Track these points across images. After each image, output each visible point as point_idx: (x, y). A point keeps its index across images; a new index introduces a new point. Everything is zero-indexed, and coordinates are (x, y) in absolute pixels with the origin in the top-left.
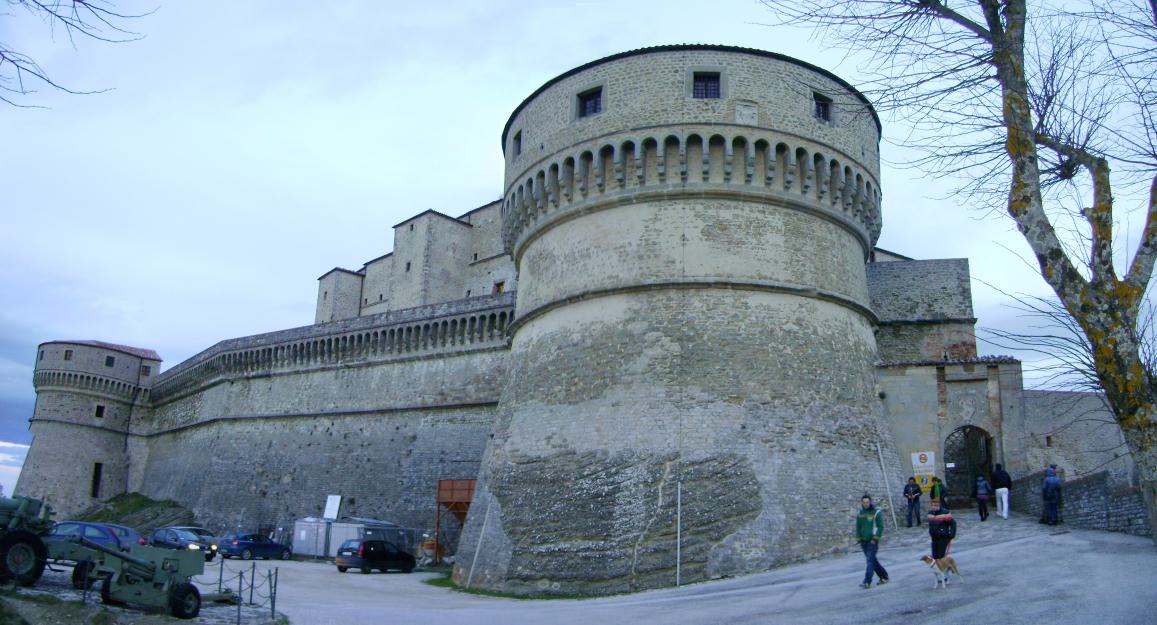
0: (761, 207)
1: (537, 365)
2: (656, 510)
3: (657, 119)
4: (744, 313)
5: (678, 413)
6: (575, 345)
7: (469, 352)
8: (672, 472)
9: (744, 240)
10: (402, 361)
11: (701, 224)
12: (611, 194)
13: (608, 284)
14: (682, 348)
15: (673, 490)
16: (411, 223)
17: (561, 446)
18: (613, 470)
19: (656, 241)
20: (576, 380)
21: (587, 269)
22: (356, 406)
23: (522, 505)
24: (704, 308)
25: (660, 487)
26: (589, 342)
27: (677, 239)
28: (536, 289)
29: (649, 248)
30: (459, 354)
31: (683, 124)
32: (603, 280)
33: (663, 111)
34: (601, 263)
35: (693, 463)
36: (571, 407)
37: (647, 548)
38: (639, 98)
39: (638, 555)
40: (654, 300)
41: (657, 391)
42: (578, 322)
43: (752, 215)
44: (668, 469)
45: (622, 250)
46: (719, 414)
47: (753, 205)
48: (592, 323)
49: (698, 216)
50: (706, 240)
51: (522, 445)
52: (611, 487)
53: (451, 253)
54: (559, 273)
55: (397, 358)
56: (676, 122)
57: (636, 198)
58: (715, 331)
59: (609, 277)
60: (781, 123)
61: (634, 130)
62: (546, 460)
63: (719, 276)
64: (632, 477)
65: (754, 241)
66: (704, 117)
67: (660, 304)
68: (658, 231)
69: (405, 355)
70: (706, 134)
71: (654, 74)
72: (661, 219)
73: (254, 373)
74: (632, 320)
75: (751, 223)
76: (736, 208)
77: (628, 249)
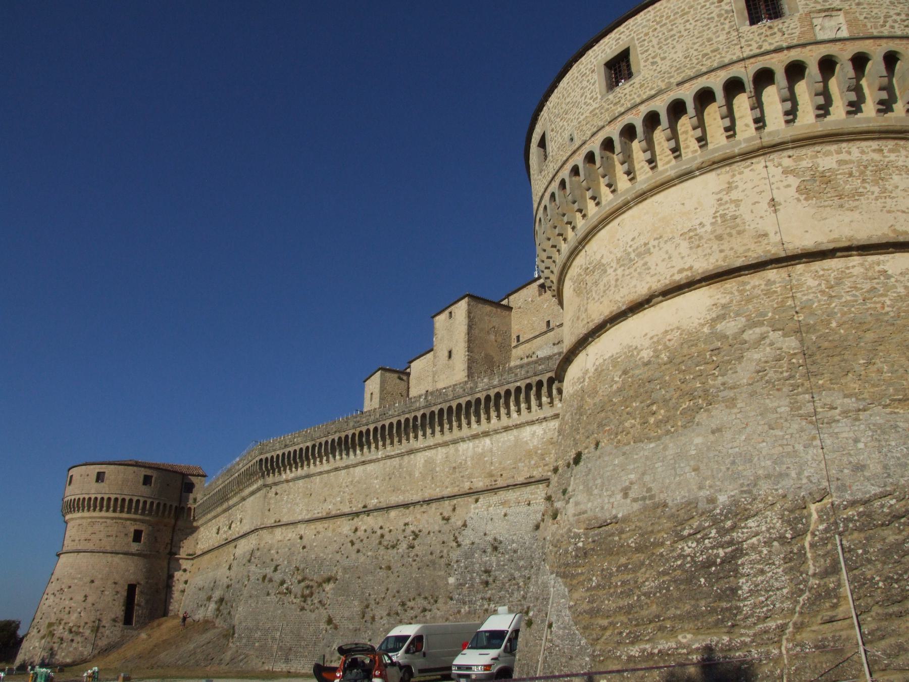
0: (874, 144)
1: (597, 400)
2: (805, 581)
3: (708, 63)
4: (885, 285)
5: (814, 432)
6: (648, 363)
7: (517, 426)
8: (821, 520)
9: (861, 190)
10: (445, 444)
11: (794, 181)
12: (666, 170)
13: (680, 278)
14: (802, 341)
15: (829, 547)
16: (449, 310)
17: (644, 499)
18: (729, 524)
19: (737, 213)
20: (654, 408)
21: (649, 269)
22: (400, 499)
23: (598, 586)
24: (823, 286)
25: (807, 545)
26: (664, 357)
27: (764, 204)
28: (586, 310)
30: (507, 429)
31: (743, 59)
32: (671, 276)
33: (713, 51)
34: (666, 256)
35: (853, 504)
36: (652, 445)
37: (802, 645)
38: (678, 46)
39: (790, 658)
40: (748, 287)
41: (776, 404)
42: (646, 335)
43: (864, 157)
44: (815, 516)
45: (691, 234)
46: (880, 427)
47: (864, 144)
48: (666, 332)
49: (786, 172)
50: (806, 199)
51: (590, 505)
52: (730, 549)
53: (492, 337)
54: (613, 282)
55: (440, 441)
56: (735, 58)
57: (698, 169)
58: (844, 314)
59: (680, 271)
60: (883, 26)
61: (679, 84)
62: (625, 520)
63: (834, 241)
64: (757, 529)
65: (876, 189)
66: (770, 44)
67: (757, 291)
68: (737, 203)
70: (778, 63)
71: (692, 12)
72: (737, 187)
73: (292, 475)
74: (721, 317)
75: (866, 167)
76: (839, 152)
77: (701, 231)
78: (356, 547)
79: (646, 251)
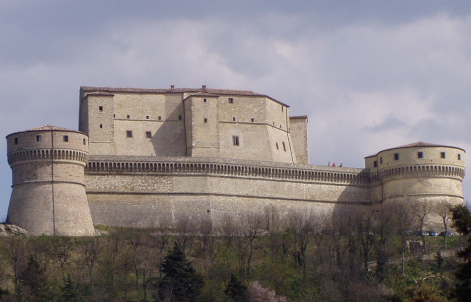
10: (297, 182)
22: (280, 196)
29: (450, 188)
30: (318, 183)
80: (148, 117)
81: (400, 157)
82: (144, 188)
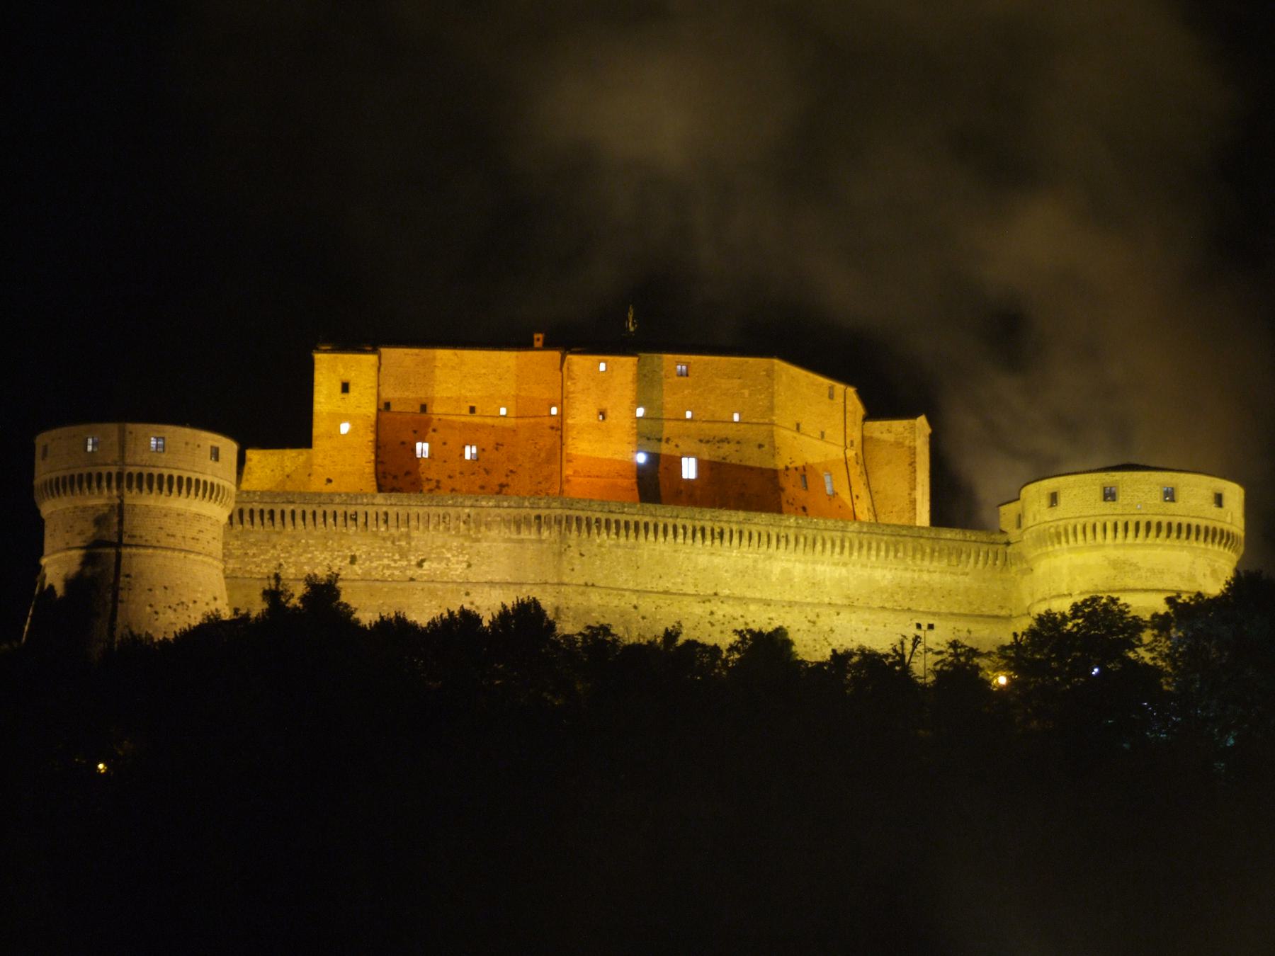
22: (758, 595)
30: (864, 566)
69: (809, 557)
78: (718, 628)
79: (1162, 572)
80: (472, 410)
81: (1062, 500)
82: (397, 573)
